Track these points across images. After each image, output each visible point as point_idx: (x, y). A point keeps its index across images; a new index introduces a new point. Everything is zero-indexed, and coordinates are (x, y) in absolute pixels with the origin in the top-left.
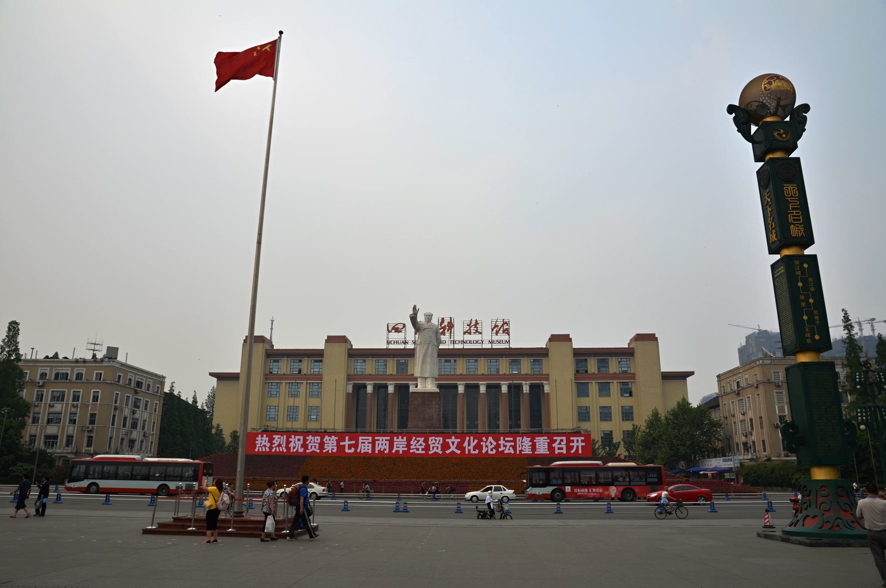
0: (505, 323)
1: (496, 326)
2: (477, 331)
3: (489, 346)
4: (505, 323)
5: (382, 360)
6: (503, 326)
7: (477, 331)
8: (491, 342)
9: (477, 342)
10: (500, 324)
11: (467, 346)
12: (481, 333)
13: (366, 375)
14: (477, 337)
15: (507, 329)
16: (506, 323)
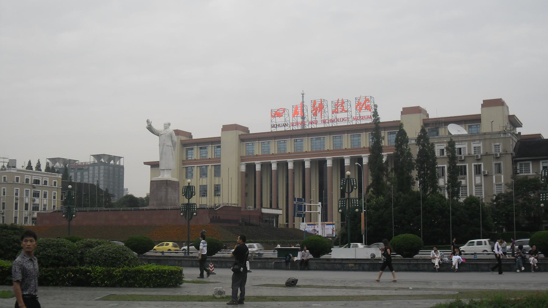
0: (367, 100)
1: (359, 104)
2: (343, 110)
3: (354, 123)
4: (367, 100)
5: (282, 140)
6: (365, 103)
7: (343, 110)
8: (356, 119)
9: (343, 119)
10: (362, 101)
11: (340, 124)
12: (347, 111)
13: (254, 156)
14: (344, 115)
15: (369, 106)
16: (368, 100)
